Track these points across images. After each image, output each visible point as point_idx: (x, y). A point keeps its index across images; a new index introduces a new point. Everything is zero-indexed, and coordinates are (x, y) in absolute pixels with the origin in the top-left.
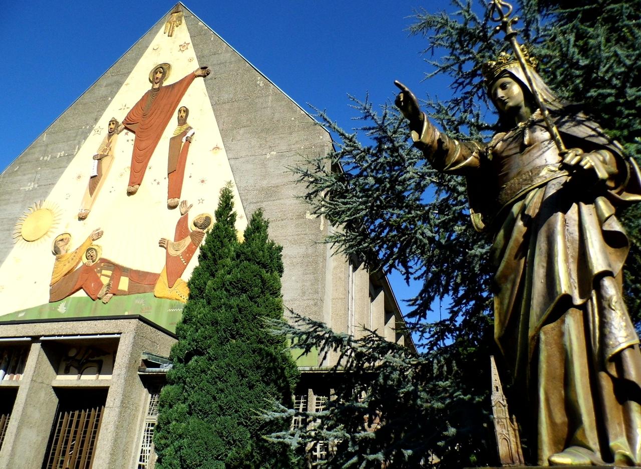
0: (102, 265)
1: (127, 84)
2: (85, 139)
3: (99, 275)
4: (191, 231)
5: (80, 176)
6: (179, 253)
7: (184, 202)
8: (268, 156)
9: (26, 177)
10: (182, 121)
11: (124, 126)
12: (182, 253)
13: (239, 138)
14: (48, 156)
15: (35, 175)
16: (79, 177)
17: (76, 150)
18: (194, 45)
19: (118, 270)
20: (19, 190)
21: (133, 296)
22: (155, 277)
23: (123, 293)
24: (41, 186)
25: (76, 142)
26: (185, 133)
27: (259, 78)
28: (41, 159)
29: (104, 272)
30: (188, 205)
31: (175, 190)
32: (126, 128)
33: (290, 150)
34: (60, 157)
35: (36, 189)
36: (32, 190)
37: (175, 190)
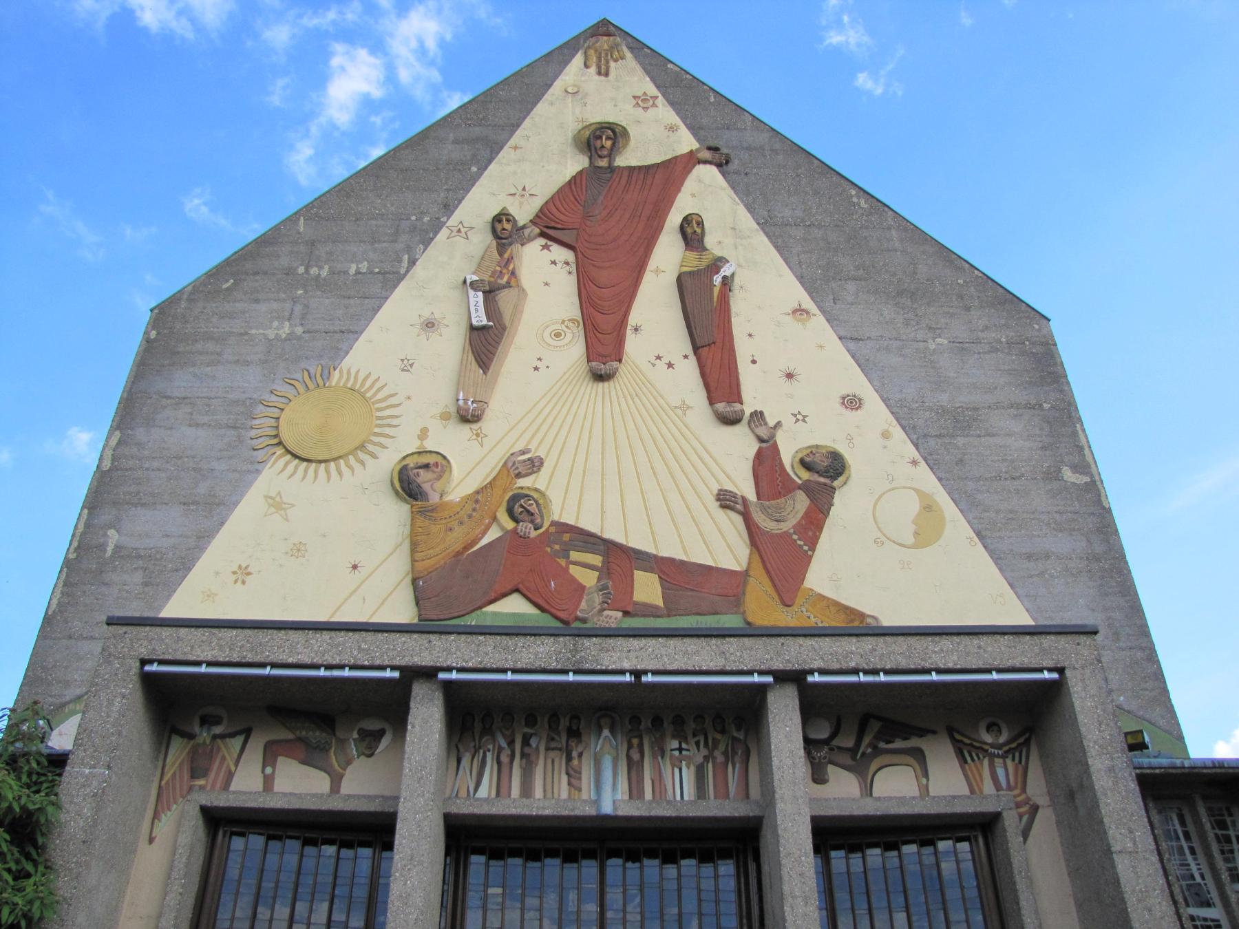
0: (566, 537)
1: (516, 148)
2: (427, 242)
3: (563, 562)
4: (800, 482)
5: (433, 325)
6: (787, 526)
7: (758, 416)
8: (932, 346)
9: (263, 307)
11: (537, 231)
12: (794, 527)
13: (850, 299)
14: (321, 268)
15: (288, 306)
20: (246, 333)
24: (316, 332)
25: (399, 246)
27: (854, 192)
29: (574, 555)
30: (771, 423)
32: (543, 235)
33: (977, 342)
34: (358, 272)
35: (299, 338)
36: (286, 340)
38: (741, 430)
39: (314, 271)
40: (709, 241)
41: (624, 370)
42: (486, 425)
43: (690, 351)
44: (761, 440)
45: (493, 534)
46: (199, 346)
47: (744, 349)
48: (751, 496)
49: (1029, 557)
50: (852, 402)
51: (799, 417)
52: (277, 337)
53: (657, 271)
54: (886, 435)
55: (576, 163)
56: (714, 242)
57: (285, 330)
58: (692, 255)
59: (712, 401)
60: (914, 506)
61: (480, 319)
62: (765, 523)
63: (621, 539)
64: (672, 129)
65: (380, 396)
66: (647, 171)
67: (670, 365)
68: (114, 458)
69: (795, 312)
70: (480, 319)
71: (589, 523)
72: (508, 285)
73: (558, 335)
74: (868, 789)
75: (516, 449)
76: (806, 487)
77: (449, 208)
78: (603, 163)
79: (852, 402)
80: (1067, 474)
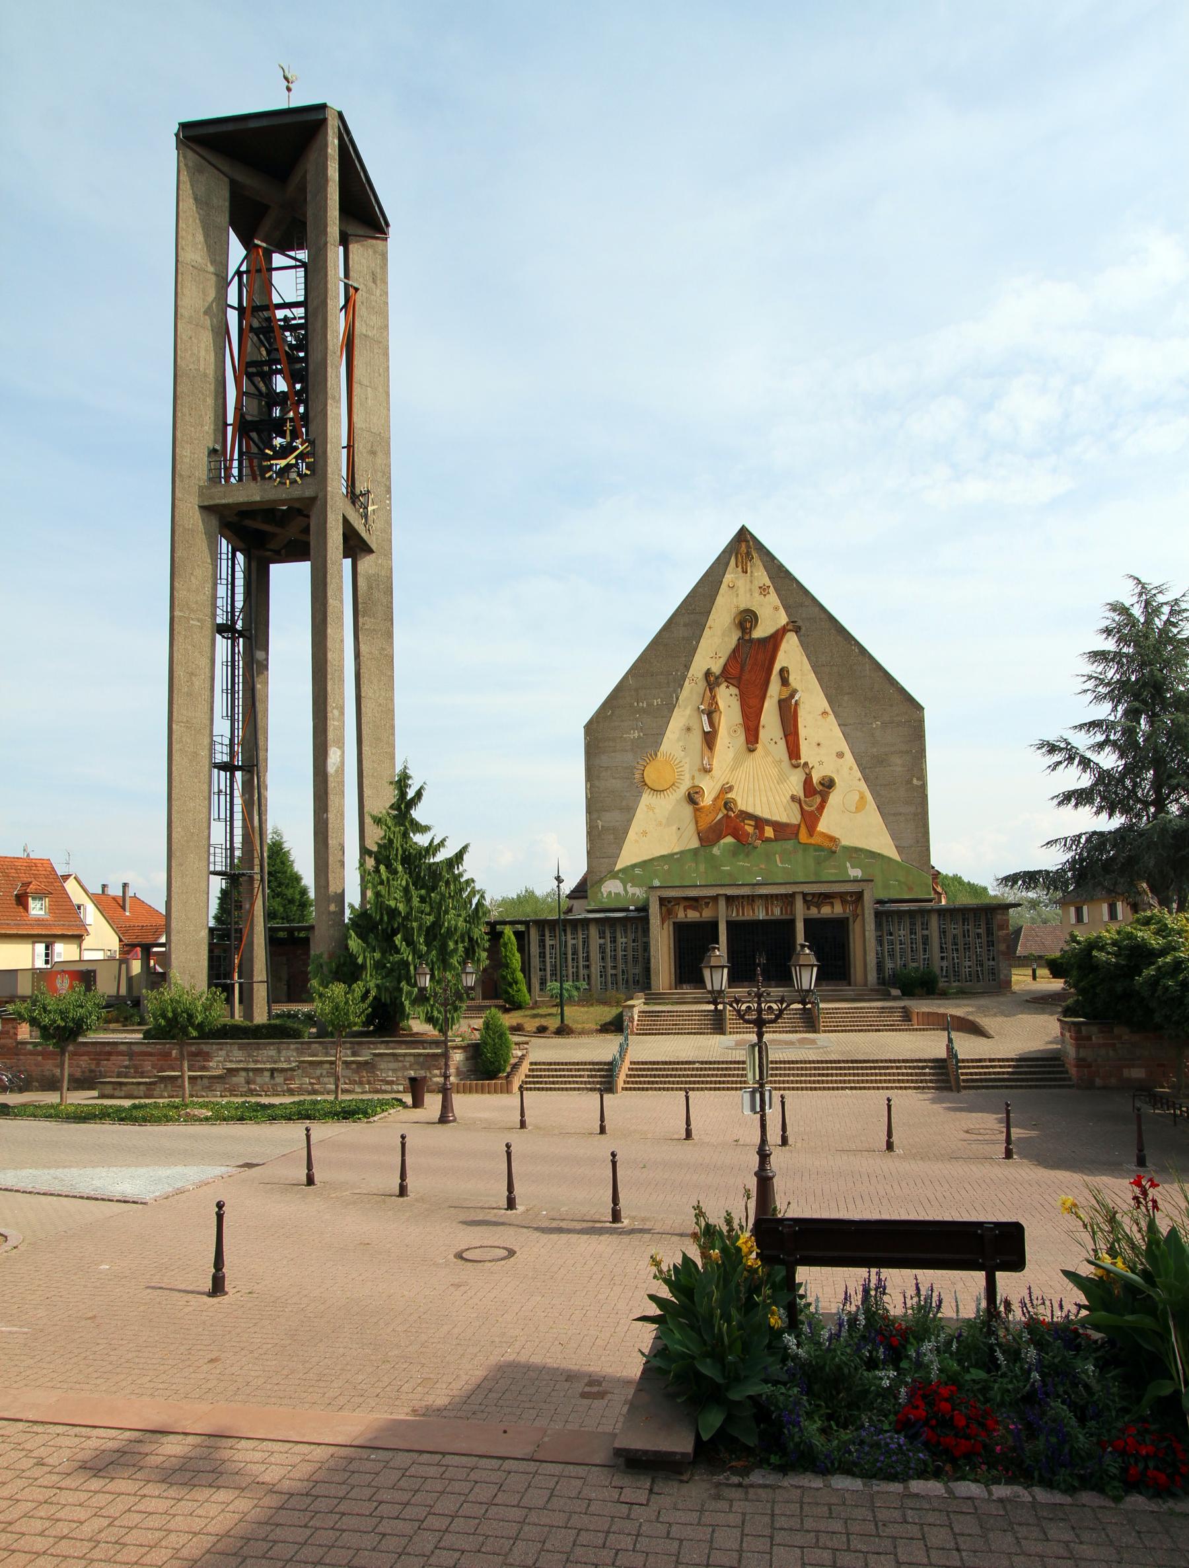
2: (681, 686)
6: (812, 808)
7: (806, 764)
10: (785, 681)
16: (689, 729)
18: (777, 590)
19: (760, 822)
21: (780, 843)
23: (768, 840)
26: (792, 696)
30: (810, 766)
31: (793, 751)
37: (793, 751)
38: (800, 769)
40: (791, 679)
42: (713, 772)
45: (720, 816)
46: (606, 744)
47: (802, 732)
49: (894, 815)
50: (840, 755)
51: (821, 763)
53: (771, 697)
54: (851, 769)
57: (636, 735)
58: (784, 688)
59: (790, 759)
60: (857, 797)
61: (707, 729)
62: (806, 808)
64: (776, 609)
66: (763, 641)
70: (707, 729)
71: (750, 810)
74: (819, 912)
76: (820, 793)
77: (687, 667)
78: (747, 637)
80: (915, 781)
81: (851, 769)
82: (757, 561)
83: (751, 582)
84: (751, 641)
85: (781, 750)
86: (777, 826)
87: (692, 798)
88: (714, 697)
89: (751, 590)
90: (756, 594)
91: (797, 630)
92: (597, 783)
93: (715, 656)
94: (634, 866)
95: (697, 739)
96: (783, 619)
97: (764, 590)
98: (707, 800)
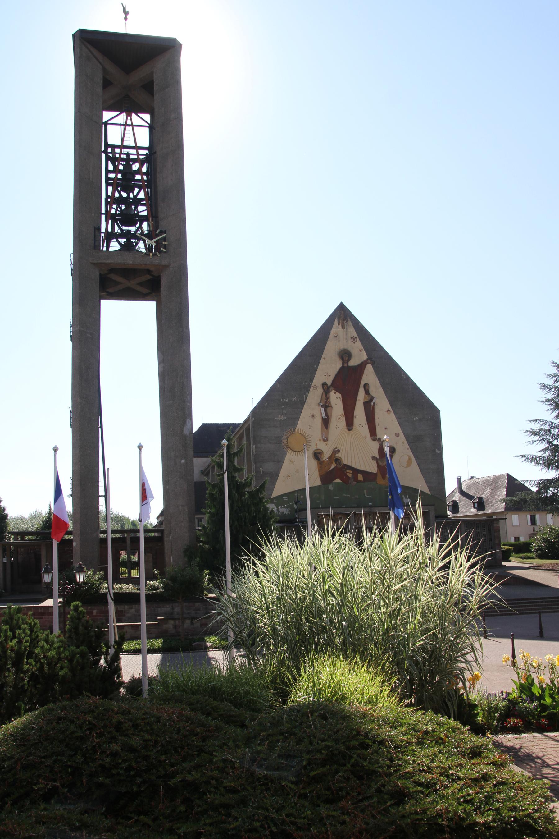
2: (308, 391)
7: (379, 439)
10: (367, 392)
16: (313, 416)
17: (304, 398)
18: (361, 341)
19: (356, 471)
22: (375, 475)
23: (361, 481)
28: (282, 400)
29: (347, 471)
38: (376, 442)
39: (285, 400)
41: (354, 427)
42: (328, 442)
43: (366, 423)
44: (380, 445)
45: (333, 467)
47: (377, 421)
48: (378, 457)
50: (397, 435)
52: (281, 419)
53: (359, 400)
54: (403, 443)
55: (338, 365)
56: (372, 392)
57: (282, 418)
60: (407, 459)
62: (381, 464)
63: (355, 467)
64: (361, 351)
65: (306, 435)
67: (362, 426)
68: (256, 451)
69: (388, 411)
71: (349, 464)
72: (328, 406)
73: (340, 419)
75: (335, 448)
77: (311, 380)
78: (345, 365)
79: (397, 435)
81: (403, 443)
82: (350, 323)
83: (347, 334)
84: (348, 367)
85: (365, 430)
86: (364, 473)
87: (317, 455)
88: (327, 398)
89: (346, 339)
90: (350, 342)
91: (373, 364)
92: (259, 445)
93: (328, 375)
94: (283, 496)
95: (318, 423)
96: (365, 357)
97: (354, 339)
98: (326, 457)
